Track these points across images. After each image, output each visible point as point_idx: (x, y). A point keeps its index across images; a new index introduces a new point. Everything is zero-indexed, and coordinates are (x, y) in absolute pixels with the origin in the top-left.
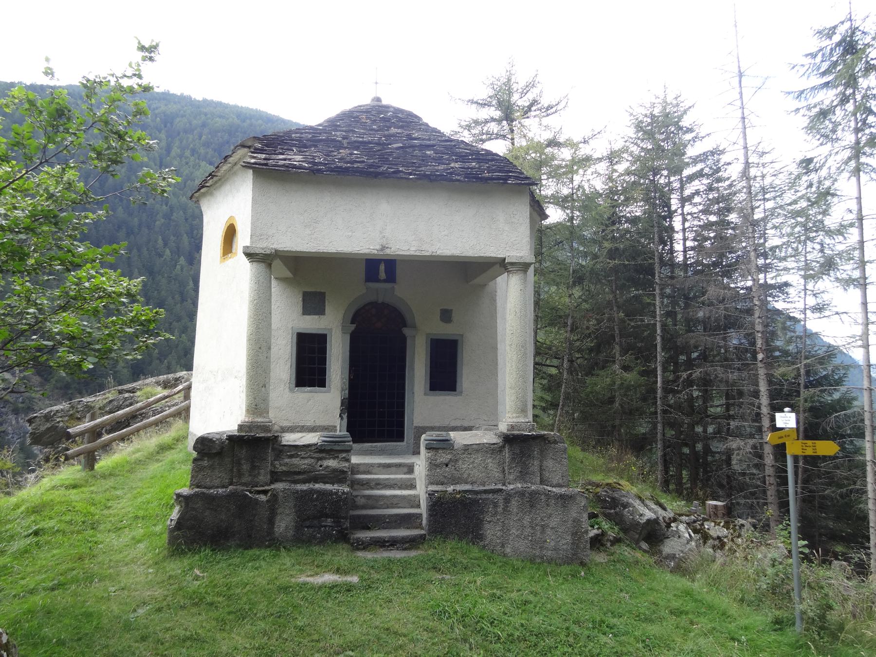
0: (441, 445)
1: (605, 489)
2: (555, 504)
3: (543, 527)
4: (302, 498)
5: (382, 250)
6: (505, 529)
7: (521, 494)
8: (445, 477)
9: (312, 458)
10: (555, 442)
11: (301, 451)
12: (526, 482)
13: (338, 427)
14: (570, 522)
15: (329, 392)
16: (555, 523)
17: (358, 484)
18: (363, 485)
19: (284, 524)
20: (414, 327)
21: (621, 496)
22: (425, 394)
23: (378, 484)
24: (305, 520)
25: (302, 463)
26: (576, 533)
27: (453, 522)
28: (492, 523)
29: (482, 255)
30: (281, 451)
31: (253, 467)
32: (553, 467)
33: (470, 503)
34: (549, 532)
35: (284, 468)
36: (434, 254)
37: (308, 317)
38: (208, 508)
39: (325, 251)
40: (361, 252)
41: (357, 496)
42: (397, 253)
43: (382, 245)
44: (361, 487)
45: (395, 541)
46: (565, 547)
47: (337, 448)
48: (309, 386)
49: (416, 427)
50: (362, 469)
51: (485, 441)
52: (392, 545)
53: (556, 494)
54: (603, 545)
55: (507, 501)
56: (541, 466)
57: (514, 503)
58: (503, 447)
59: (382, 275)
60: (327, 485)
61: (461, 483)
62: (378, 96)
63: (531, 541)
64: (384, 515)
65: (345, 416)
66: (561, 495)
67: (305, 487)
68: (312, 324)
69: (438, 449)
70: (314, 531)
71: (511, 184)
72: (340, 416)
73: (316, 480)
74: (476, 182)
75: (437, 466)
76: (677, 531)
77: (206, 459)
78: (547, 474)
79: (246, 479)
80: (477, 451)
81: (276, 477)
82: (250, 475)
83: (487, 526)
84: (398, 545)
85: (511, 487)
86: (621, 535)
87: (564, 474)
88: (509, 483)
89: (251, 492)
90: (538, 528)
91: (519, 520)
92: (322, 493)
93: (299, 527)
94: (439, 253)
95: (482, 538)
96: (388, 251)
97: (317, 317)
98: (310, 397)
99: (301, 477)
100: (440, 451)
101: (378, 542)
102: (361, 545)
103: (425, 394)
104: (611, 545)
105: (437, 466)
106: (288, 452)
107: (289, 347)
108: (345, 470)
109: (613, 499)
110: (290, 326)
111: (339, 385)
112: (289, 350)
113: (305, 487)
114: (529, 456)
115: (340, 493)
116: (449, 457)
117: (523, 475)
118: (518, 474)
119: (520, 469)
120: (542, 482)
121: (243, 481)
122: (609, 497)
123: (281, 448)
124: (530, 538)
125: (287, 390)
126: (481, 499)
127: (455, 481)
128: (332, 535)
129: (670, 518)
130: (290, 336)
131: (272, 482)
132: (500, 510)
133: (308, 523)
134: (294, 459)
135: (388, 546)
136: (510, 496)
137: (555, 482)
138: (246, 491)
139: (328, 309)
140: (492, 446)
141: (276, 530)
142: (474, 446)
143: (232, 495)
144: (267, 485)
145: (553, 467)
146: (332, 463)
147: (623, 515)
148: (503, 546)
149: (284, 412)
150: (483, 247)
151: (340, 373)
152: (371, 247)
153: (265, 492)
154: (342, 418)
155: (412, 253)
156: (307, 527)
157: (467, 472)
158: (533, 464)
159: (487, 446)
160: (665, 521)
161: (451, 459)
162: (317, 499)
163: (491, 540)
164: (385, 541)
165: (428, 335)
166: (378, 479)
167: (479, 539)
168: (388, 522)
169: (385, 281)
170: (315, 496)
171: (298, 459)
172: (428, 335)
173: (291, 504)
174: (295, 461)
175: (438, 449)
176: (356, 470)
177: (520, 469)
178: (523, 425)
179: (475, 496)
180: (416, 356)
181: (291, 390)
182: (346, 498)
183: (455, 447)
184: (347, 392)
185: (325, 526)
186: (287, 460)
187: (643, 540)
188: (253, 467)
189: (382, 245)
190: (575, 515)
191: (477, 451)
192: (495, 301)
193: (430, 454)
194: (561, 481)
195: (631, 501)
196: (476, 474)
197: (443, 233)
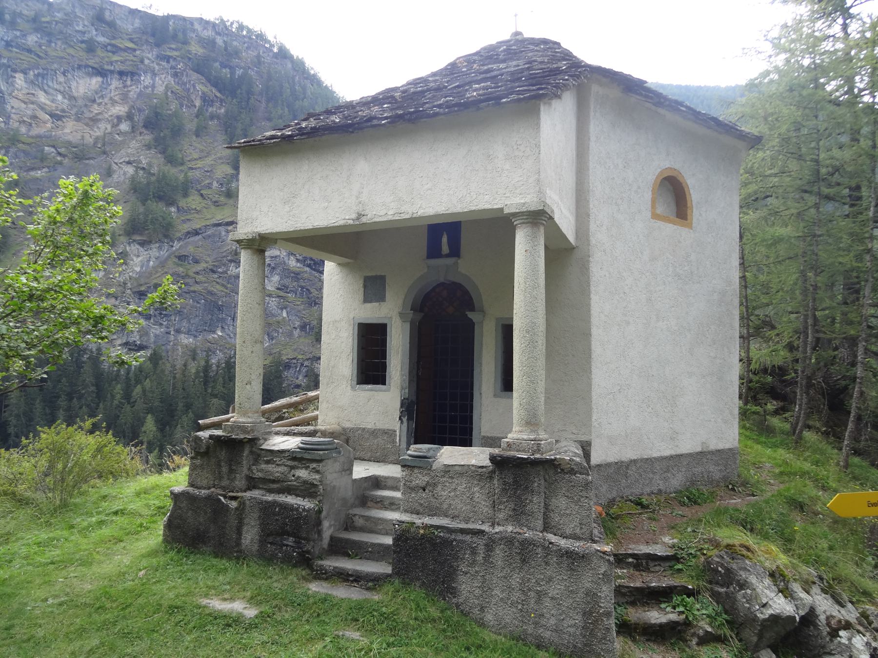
0: (417, 463)
1: (722, 553)
2: (557, 563)
3: (540, 595)
4: (267, 509)
5: (358, 219)
6: (486, 588)
7: (509, 541)
8: (421, 505)
9: (286, 466)
10: (572, 472)
11: (276, 457)
12: (521, 525)
13: (398, 431)
14: (581, 595)
15: (388, 390)
16: (556, 591)
17: (372, 501)
18: (377, 502)
19: (250, 536)
20: (482, 311)
21: (741, 569)
22: (495, 396)
23: (392, 504)
24: (268, 535)
25: (276, 470)
26: (591, 613)
27: (420, 564)
28: (468, 575)
29: (473, 208)
30: (259, 455)
31: (231, 471)
32: (567, 508)
33: (441, 542)
34: (547, 602)
35: (260, 475)
36: (415, 216)
37: (369, 305)
38: (191, 509)
39: (302, 228)
40: (336, 224)
41: (355, 515)
42: (373, 220)
43: (358, 213)
44: (375, 505)
45: (359, 577)
46: (572, 630)
47: (307, 456)
48: (374, 384)
49: (484, 437)
50: (390, 483)
51: (473, 462)
52: (355, 581)
53: (560, 550)
54: (685, 641)
55: (490, 547)
56: (546, 506)
57: (499, 552)
58: (493, 472)
59: (445, 249)
60: (289, 497)
61: (439, 516)
62: (519, 30)
63: (521, 610)
64: (367, 543)
65: (405, 419)
66: (567, 552)
67: (270, 498)
68: (372, 313)
69: (414, 467)
70: (276, 549)
71: (505, 102)
72: (400, 419)
73: (289, 491)
74: (458, 110)
75: (413, 489)
76: (849, 647)
77: (199, 458)
78: (555, 518)
79: (225, 482)
80: (461, 474)
81: (252, 483)
82: (228, 479)
83: (462, 578)
84: (362, 582)
85: (498, 529)
86: (726, 631)
87: (584, 522)
88: (498, 524)
89: (225, 497)
90: (532, 594)
91: (505, 578)
92: (285, 507)
93: (263, 542)
94: (421, 213)
95: (455, 593)
96: (364, 220)
97: (376, 304)
98: (370, 394)
99: (275, 486)
100: (416, 471)
101: (342, 574)
102: (325, 574)
103: (495, 396)
104: (698, 644)
105: (413, 489)
106: (265, 457)
107: (351, 340)
108: (315, 483)
109: (728, 571)
110: (351, 316)
111: (399, 381)
112: (351, 344)
113: (270, 498)
114: (527, 488)
115: (301, 510)
116: (426, 479)
117: (519, 515)
118: (510, 513)
119: (513, 506)
120: (546, 528)
121: (223, 485)
122: (722, 566)
123: (259, 452)
124: (520, 607)
125: (349, 388)
126: (455, 540)
127: (433, 512)
128: (293, 557)
129: (840, 621)
130: (351, 328)
131: (249, 489)
132: (480, 558)
133: (271, 539)
134: (270, 465)
135: (352, 582)
136: (494, 541)
137: (568, 532)
138: (221, 495)
139: (389, 295)
140: (480, 470)
141: (243, 541)
142: (457, 468)
143: (208, 498)
144: (242, 491)
145: (567, 508)
146: (303, 473)
147: (735, 600)
148: (482, 609)
149: (346, 412)
150: (475, 197)
151: (399, 369)
152: (347, 217)
153: (234, 498)
154: (402, 423)
155: (390, 218)
156: (271, 543)
157: (447, 501)
158: (531, 501)
159: (473, 468)
160: (828, 624)
161: (428, 482)
162: (279, 514)
163: (467, 599)
164: (349, 575)
165: (497, 319)
166: (392, 498)
167: (451, 594)
168: (371, 552)
169: (447, 256)
170: (277, 510)
171: (273, 466)
172: (497, 319)
173: (256, 515)
174: (270, 467)
175: (414, 467)
176: (383, 484)
177: (513, 506)
178: (524, 444)
179: (448, 535)
180: (484, 347)
181: (353, 388)
182: (306, 516)
183: (434, 467)
184: (407, 391)
185: (287, 545)
186: (263, 466)
187: (769, 647)
188: (231, 471)
189: (358, 213)
190: (588, 585)
191: (461, 474)
192: (588, 269)
193: (404, 473)
194: (578, 531)
195: (753, 579)
196: (459, 505)
197: (426, 187)
